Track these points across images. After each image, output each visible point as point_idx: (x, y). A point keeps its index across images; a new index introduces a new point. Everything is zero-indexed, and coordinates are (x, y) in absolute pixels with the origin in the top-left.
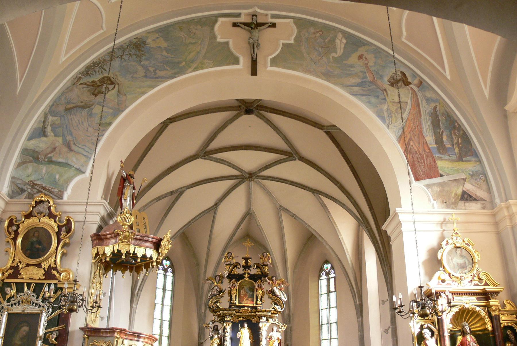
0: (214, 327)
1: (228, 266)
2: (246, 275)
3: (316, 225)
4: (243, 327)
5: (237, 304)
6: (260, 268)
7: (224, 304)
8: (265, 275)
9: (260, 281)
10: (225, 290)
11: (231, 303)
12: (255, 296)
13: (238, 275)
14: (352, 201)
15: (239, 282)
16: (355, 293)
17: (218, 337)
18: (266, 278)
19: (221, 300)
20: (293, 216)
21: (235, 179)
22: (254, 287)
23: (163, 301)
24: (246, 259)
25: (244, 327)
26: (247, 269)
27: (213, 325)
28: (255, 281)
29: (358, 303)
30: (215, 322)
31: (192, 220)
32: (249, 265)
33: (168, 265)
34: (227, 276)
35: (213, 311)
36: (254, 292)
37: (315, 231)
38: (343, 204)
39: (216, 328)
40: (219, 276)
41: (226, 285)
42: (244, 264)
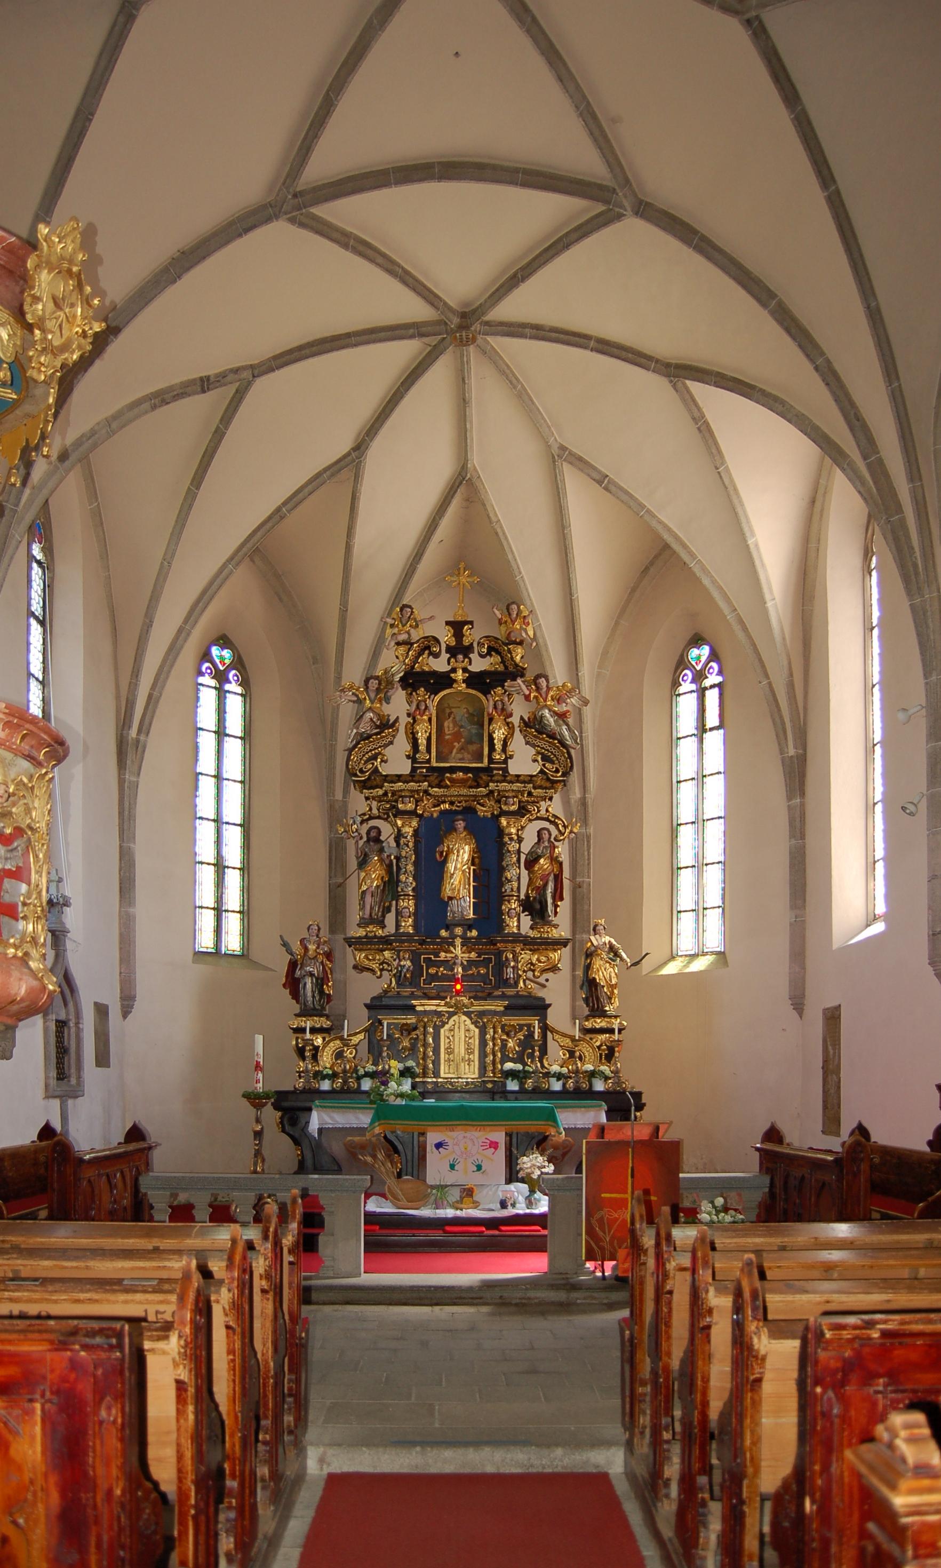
0: (368, 833)
1: (402, 650)
2: (459, 676)
3: (678, 512)
4: (452, 829)
5: (434, 764)
6: (498, 653)
7: (396, 760)
8: (513, 672)
9: (499, 690)
10: (397, 720)
11: (414, 760)
12: (486, 739)
13: (434, 674)
14: (820, 361)
15: (438, 698)
16: (783, 723)
17: (381, 860)
18: (519, 681)
19: (388, 751)
20: (600, 482)
21: (412, 337)
22: (481, 710)
23: (219, 767)
24: (457, 627)
25: (455, 830)
26: (460, 657)
27: (365, 827)
28: (486, 693)
29: (792, 752)
30: (371, 818)
31: (285, 503)
32: (466, 642)
33: (227, 662)
34: (402, 679)
35: (364, 785)
36: (482, 726)
37: (669, 530)
38: (776, 399)
39: (373, 834)
40: (377, 678)
41: (398, 705)
42: (453, 643)
